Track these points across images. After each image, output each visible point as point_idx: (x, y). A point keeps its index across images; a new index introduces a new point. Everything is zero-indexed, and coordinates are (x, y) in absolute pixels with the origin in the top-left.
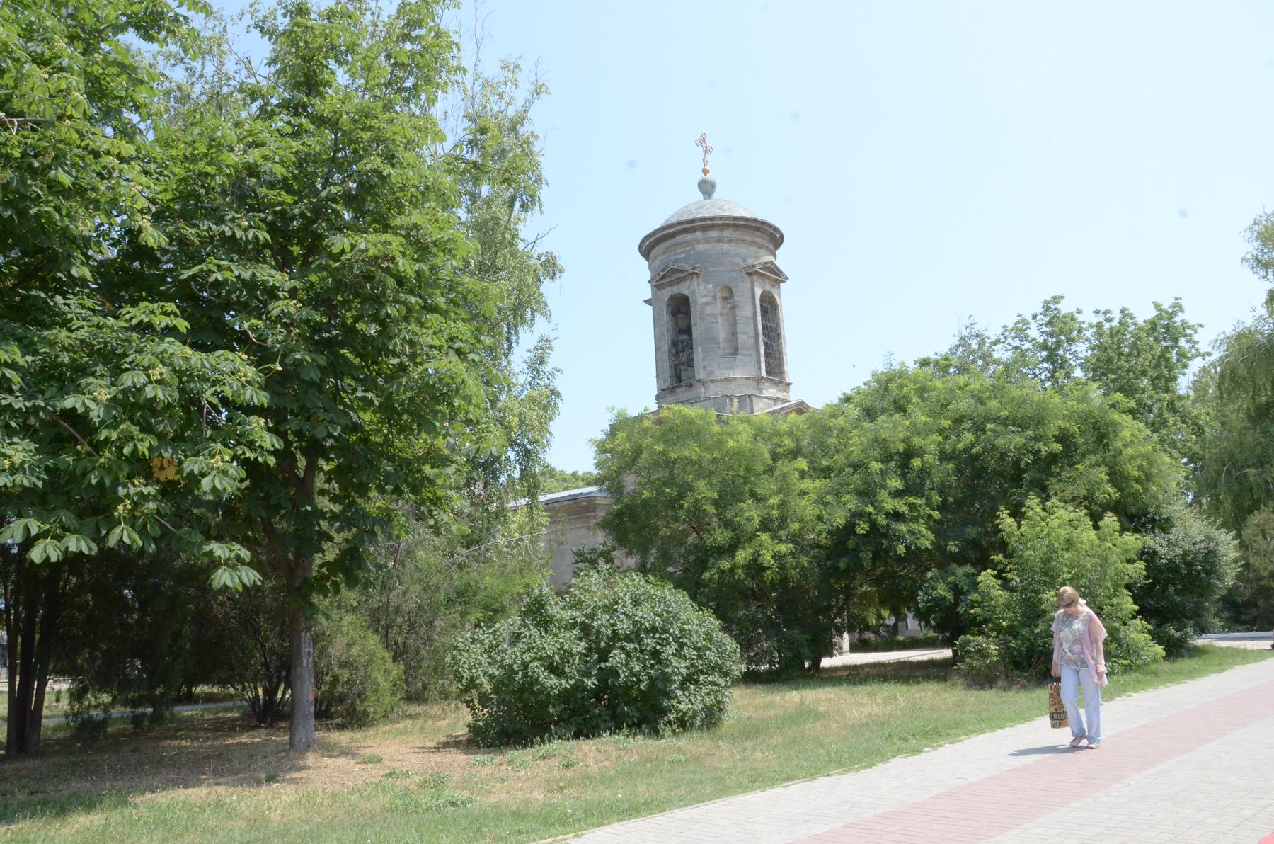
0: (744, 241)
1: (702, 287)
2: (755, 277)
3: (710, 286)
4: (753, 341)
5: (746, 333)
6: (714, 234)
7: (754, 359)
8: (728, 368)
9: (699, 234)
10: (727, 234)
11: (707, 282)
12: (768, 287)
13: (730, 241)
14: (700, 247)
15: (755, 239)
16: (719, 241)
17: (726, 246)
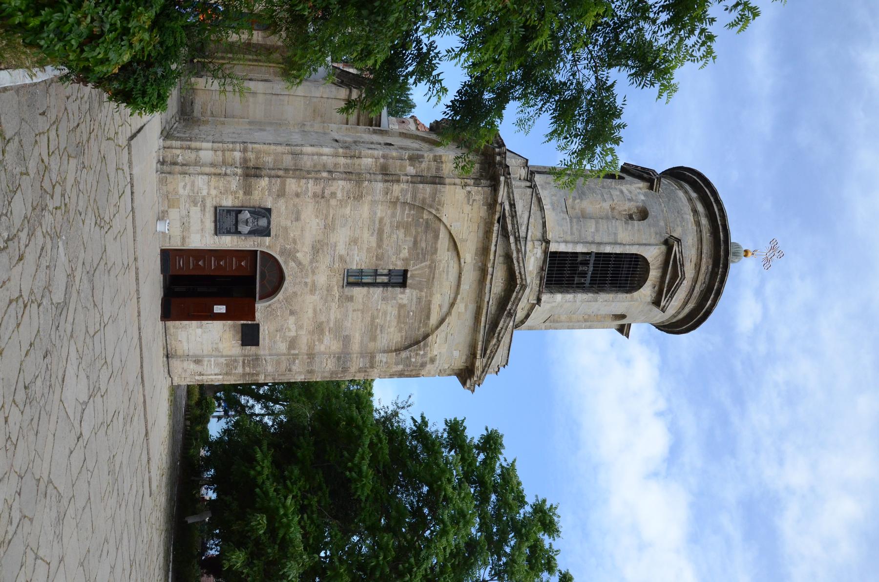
0: (701, 240)
1: (638, 191)
2: (663, 248)
3: (643, 198)
4: (590, 239)
5: (597, 230)
6: (700, 208)
7: (569, 238)
8: (553, 204)
9: (694, 195)
10: (704, 221)
11: (645, 195)
12: (654, 274)
13: (698, 224)
14: (681, 194)
15: (704, 260)
16: (695, 211)
17: (690, 217)
